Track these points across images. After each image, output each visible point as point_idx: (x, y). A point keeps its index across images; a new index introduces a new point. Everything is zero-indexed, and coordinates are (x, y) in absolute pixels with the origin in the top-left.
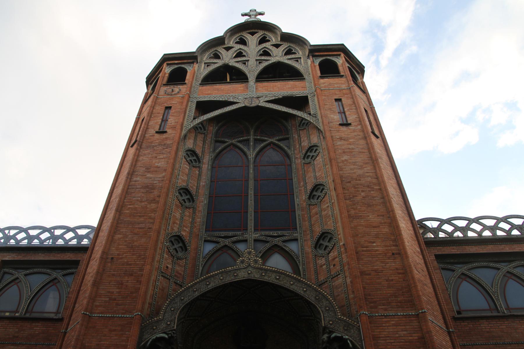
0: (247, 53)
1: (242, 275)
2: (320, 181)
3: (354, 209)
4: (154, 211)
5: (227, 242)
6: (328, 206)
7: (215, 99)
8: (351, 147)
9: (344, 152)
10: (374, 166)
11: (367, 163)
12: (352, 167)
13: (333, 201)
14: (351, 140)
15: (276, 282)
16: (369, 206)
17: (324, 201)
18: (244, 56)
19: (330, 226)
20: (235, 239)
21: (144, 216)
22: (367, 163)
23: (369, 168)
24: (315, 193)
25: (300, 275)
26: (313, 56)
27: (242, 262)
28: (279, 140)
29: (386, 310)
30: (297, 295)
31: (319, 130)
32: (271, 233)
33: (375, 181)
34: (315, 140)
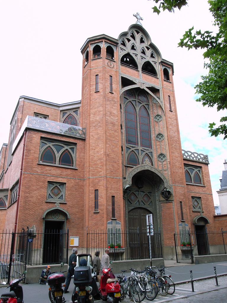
0: (136, 48)
1: (146, 168)
2: (162, 133)
3: (173, 149)
4: (117, 136)
7: (128, 78)
8: (172, 122)
9: (170, 124)
10: (178, 134)
11: (176, 131)
12: (172, 132)
13: (166, 144)
14: (172, 119)
15: (154, 172)
16: (176, 149)
17: (163, 142)
18: (135, 49)
19: (164, 152)
21: (114, 138)
22: (176, 131)
23: (176, 134)
24: (158, 136)
25: (153, 166)
26: (162, 65)
27: (146, 163)
28: (145, 105)
29: (178, 184)
30: (159, 176)
31: (162, 109)
34: (160, 113)
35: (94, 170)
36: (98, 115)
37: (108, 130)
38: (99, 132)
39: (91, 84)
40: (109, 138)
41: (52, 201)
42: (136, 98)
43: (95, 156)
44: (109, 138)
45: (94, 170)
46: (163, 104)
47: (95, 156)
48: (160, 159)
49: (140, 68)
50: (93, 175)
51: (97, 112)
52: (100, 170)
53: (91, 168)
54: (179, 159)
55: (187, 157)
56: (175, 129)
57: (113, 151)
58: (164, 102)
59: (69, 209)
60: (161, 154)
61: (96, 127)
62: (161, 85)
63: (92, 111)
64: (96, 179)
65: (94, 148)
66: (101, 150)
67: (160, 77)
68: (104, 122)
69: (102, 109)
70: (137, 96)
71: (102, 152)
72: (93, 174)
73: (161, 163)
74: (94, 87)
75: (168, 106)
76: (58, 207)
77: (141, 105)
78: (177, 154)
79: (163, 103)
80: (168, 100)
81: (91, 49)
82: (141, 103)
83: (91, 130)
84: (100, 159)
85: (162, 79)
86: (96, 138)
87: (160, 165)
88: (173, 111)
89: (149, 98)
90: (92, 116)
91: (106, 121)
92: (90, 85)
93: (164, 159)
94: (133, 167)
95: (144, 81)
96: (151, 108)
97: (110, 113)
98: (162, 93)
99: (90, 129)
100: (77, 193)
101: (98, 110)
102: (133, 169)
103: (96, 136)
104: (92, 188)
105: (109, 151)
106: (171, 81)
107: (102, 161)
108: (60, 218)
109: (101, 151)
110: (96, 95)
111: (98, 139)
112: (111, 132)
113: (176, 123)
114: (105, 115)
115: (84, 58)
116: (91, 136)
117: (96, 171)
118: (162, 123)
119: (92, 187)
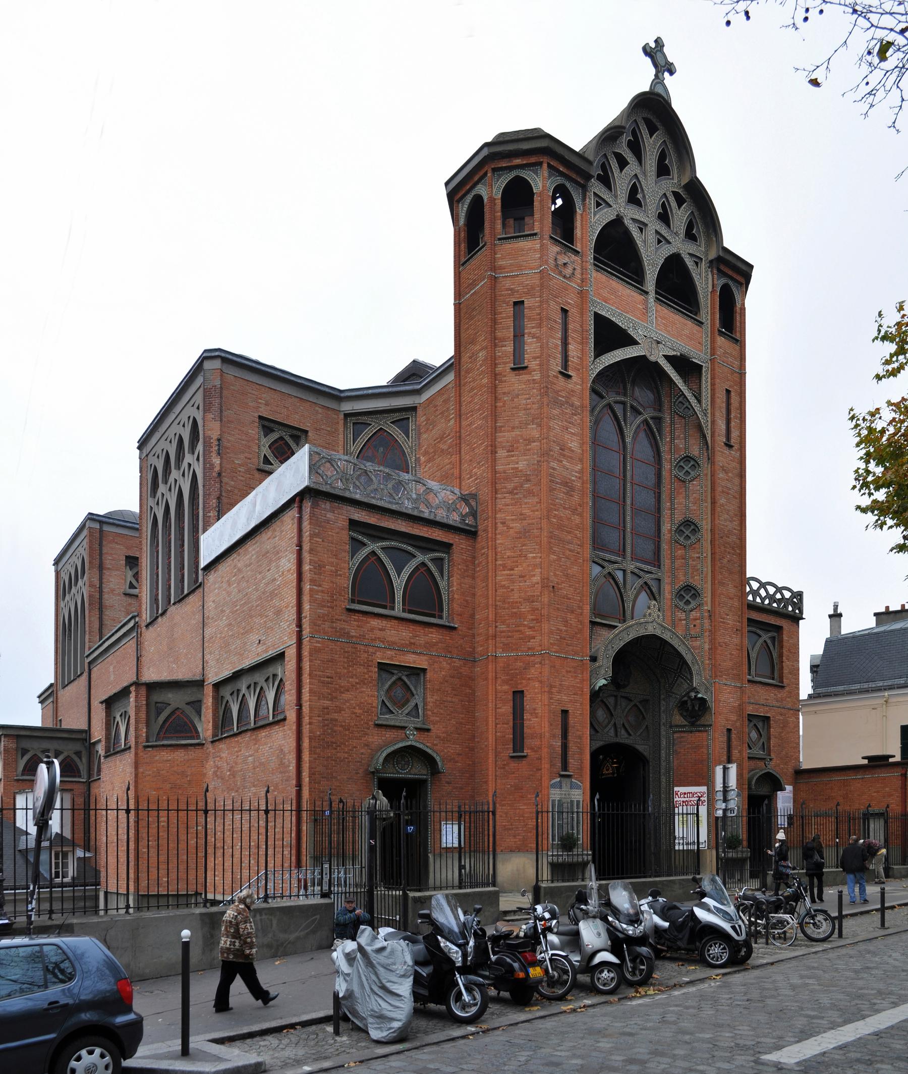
5: (610, 568)
6: (699, 558)
16: (731, 573)
19: (696, 582)
20: (616, 566)
32: (643, 566)
33: (738, 541)
35: (509, 631)
36: (525, 454)
37: (555, 505)
38: (526, 511)
39: (499, 334)
40: (556, 532)
41: (392, 723)
42: (625, 395)
43: (513, 590)
44: (556, 532)
45: (509, 631)
46: (709, 419)
47: (513, 590)
48: (681, 600)
49: (650, 284)
50: (507, 647)
51: (518, 442)
52: (529, 633)
53: (503, 627)
54: (736, 604)
55: (763, 599)
56: (733, 507)
57: (567, 576)
58: (713, 415)
59: (436, 745)
60: (688, 588)
61: (517, 494)
62: (709, 350)
63: (504, 437)
64: (516, 659)
65: (509, 563)
66: (533, 570)
67: (709, 318)
68: (544, 481)
69: (536, 434)
70: (629, 386)
71: (537, 579)
72: (508, 644)
73: (683, 616)
74: (509, 348)
75: (721, 425)
76: (413, 739)
77: (640, 419)
78: (732, 590)
79: (709, 415)
80: (724, 405)
81: (492, 191)
82: (640, 413)
83: (500, 504)
84: (530, 600)
85: (713, 325)
86: (516, 532)
87: (681, 620)
88: (736, 447)
89: (664, 392)
90: (501, 453)
91: (551, 475)
92: (495, 339)
93: (693, 604)
94: (615, 627)
95: (661, 334)
96: (666, 430)
97: (561, 449)
98: (709, 380)
99: (496, 498)
100: (455, 700)
101: (521, 436)
102: (616, 631)
103: (517, 525)
104: (506, 687)
105: (555, 575)
106: (738, 337)
107: (536, 605)
108: (414, 771)
109: (534, 575)
110: (514, 382)
111: (524, 534)
112: (563, 513)
113: (737, 488)
114: (546, 454)
115: (462, 222)
116: (499, 525)
117: (517, 635)
118: (698, 487)
119: (505, 682)
